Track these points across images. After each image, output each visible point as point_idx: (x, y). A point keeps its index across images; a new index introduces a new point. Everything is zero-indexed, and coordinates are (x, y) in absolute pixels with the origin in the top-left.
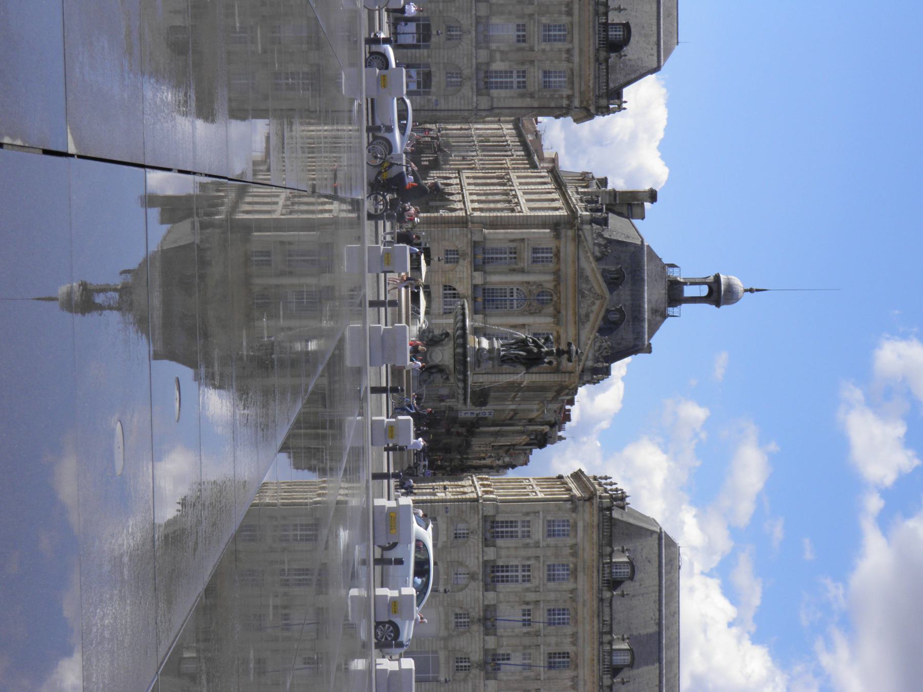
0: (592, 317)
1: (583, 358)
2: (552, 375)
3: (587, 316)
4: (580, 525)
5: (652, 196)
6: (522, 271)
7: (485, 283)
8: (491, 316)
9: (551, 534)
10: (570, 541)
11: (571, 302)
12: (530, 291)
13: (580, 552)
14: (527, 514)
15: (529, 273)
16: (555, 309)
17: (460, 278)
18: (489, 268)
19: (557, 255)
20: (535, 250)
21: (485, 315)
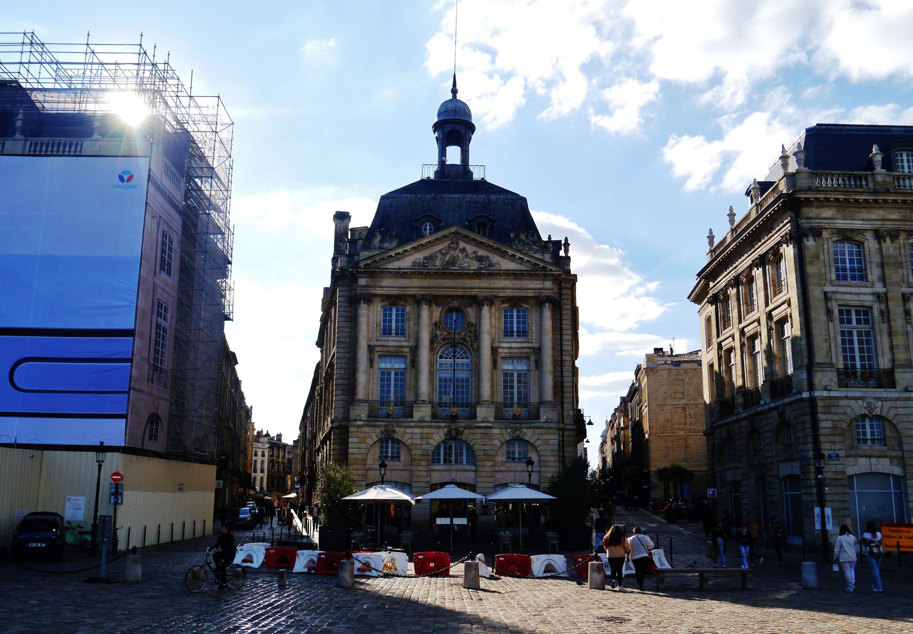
0: (482, 253)
1: (541, 264)
2: (564, 312)
3: (480, 259)
4: (841, 223)
5: (342, 217)
6: (415, 350)
7: (431, 402)
8: (479, 395)
9: (861, 275)
10: (871, 244)
11: (460, 283)
12: (443, 339)
13: (889, 225)
14: (829, 312)
15: (418, 340)
16: (470, 305)
17: (422, 438)
18: (409, 397)
19: (392, 300)
20: (387, 332)
21: (479, 403)
